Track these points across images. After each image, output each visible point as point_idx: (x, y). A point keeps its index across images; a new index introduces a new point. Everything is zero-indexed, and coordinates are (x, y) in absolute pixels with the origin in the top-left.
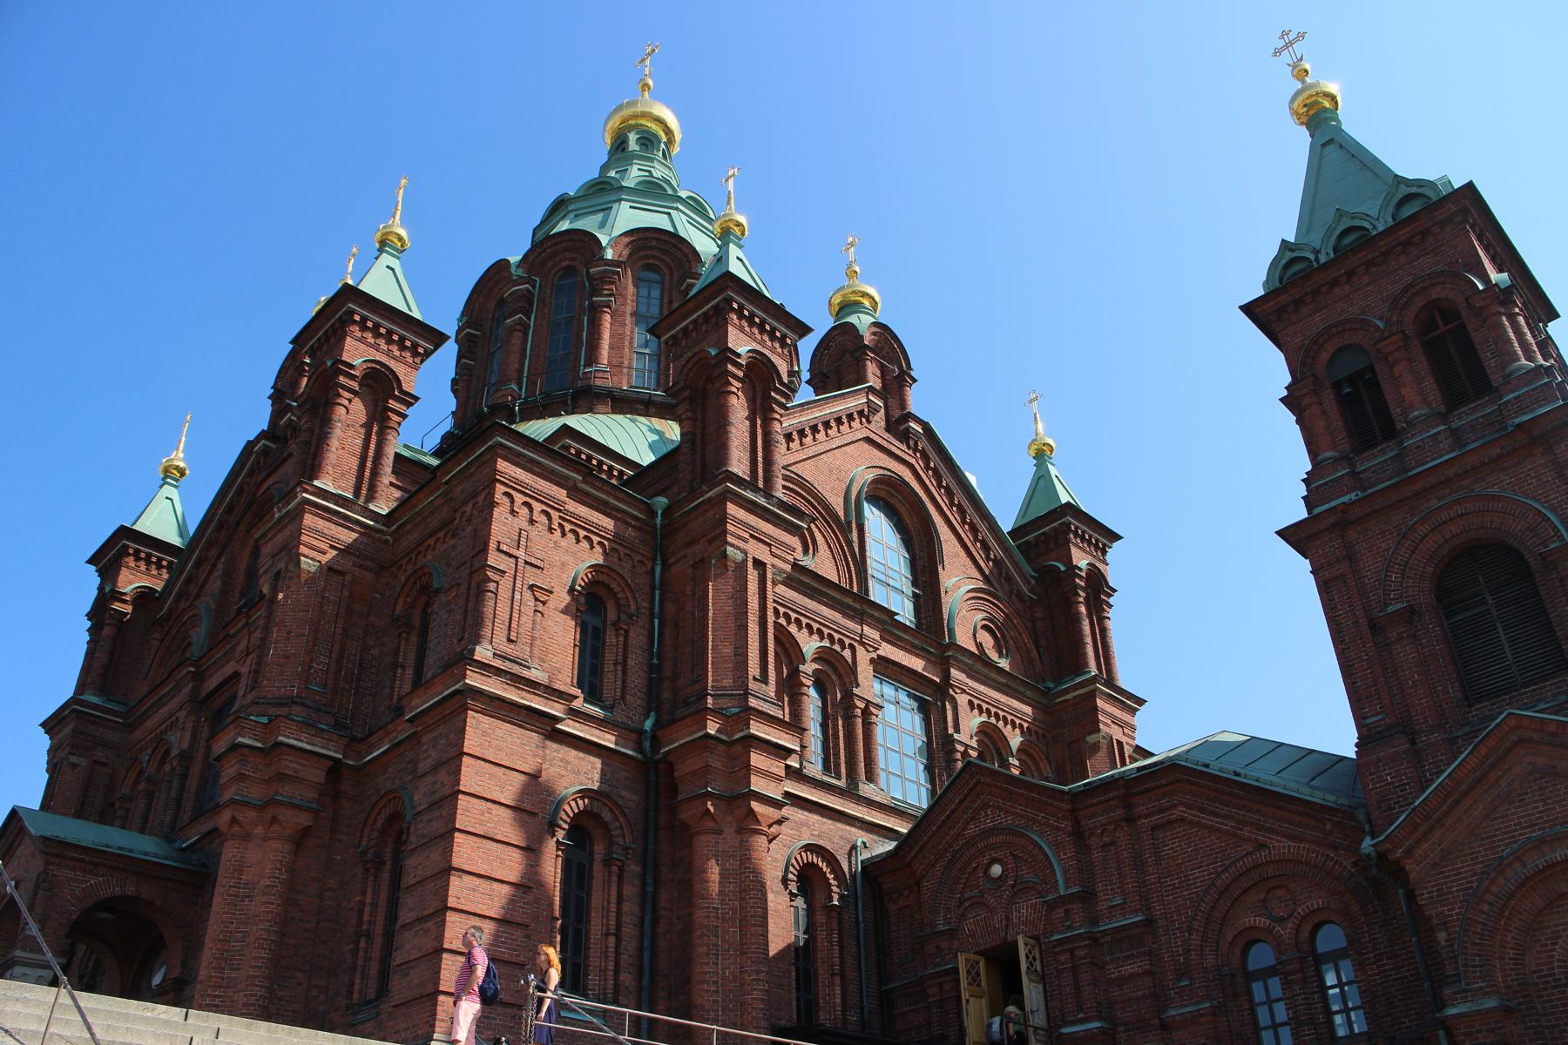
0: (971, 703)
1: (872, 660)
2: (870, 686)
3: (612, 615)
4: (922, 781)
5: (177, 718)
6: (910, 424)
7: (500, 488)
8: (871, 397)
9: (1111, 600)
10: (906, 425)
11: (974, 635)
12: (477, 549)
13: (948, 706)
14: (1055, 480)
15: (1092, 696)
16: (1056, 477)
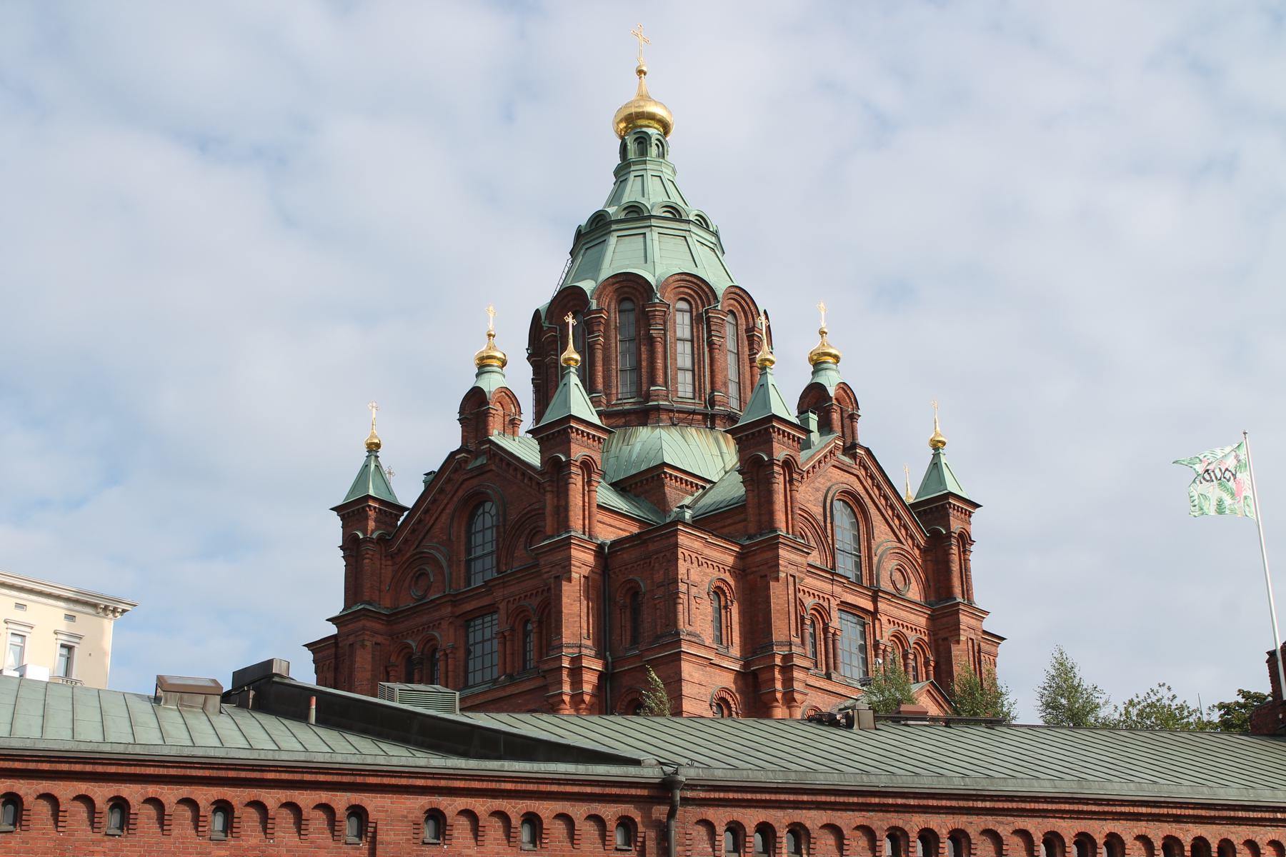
0: (889, 620)
1: (838, 605)
2: (836, 620)
3: (723, 603)
4: (861, 666)
5: (440, 624)
6: (858, 451)
7: (680, 550)
8: (836, 441)
9: (972, 548)
10: (854, 451)
11: (891, 574)
12: (671, 581)
13: (877, 626)
14: (944, 465)
15: (957, 612)
16: (946, 464)
